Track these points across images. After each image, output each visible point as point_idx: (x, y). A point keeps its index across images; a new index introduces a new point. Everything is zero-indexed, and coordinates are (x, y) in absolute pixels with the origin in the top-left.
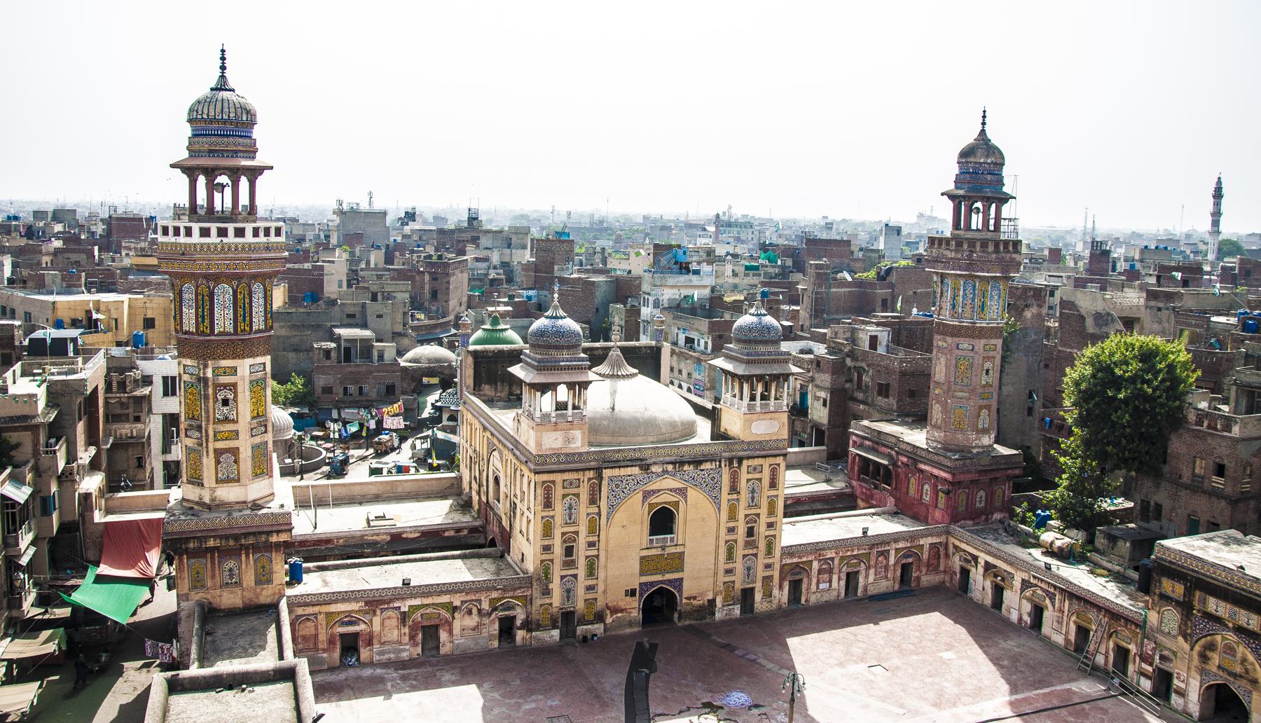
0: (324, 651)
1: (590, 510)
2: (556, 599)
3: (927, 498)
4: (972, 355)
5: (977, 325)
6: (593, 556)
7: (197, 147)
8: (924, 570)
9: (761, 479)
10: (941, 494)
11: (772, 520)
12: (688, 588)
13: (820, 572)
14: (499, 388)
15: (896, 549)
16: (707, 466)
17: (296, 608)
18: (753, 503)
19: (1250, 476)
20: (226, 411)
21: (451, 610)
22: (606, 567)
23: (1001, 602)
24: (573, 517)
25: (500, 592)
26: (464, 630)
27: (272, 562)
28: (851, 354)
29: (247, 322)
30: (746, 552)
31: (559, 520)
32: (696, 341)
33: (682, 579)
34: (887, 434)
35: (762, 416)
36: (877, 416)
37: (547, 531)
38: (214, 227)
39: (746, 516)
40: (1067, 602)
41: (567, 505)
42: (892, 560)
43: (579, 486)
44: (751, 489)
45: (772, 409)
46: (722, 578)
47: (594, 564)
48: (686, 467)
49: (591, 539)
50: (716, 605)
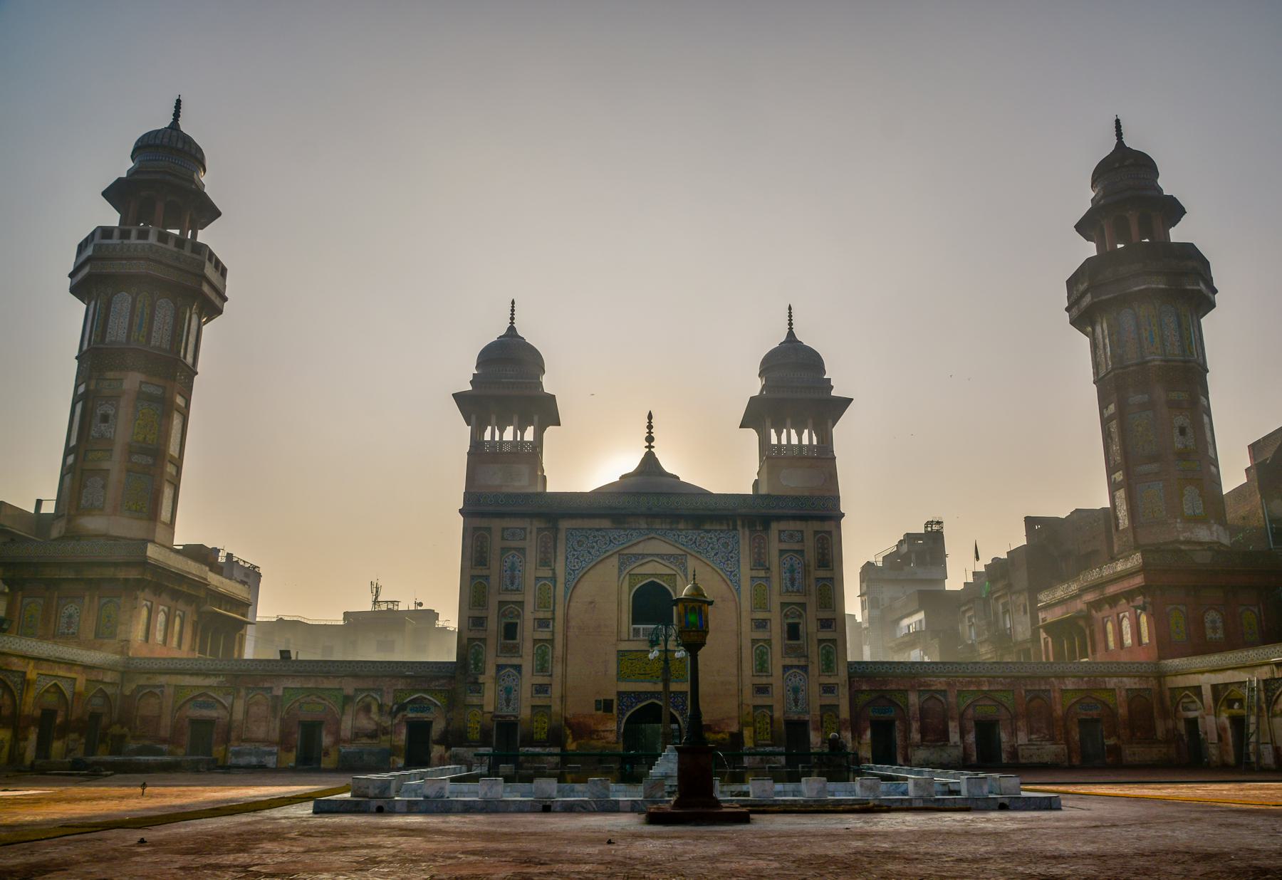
0: (164, 741)
1: (540, 574)
3: (1128, 640)
6: (546, 640)
11: (825, 615)
15: (1062, 690)
22: (564, 660)
24: (516, 584)
25: (409, 681)
30: (788, 662)
39: (783, 605)
41: (509, 564)
43: (525, 539)
44: (787, 566)
46: (750, 699)
49: (541, 615)
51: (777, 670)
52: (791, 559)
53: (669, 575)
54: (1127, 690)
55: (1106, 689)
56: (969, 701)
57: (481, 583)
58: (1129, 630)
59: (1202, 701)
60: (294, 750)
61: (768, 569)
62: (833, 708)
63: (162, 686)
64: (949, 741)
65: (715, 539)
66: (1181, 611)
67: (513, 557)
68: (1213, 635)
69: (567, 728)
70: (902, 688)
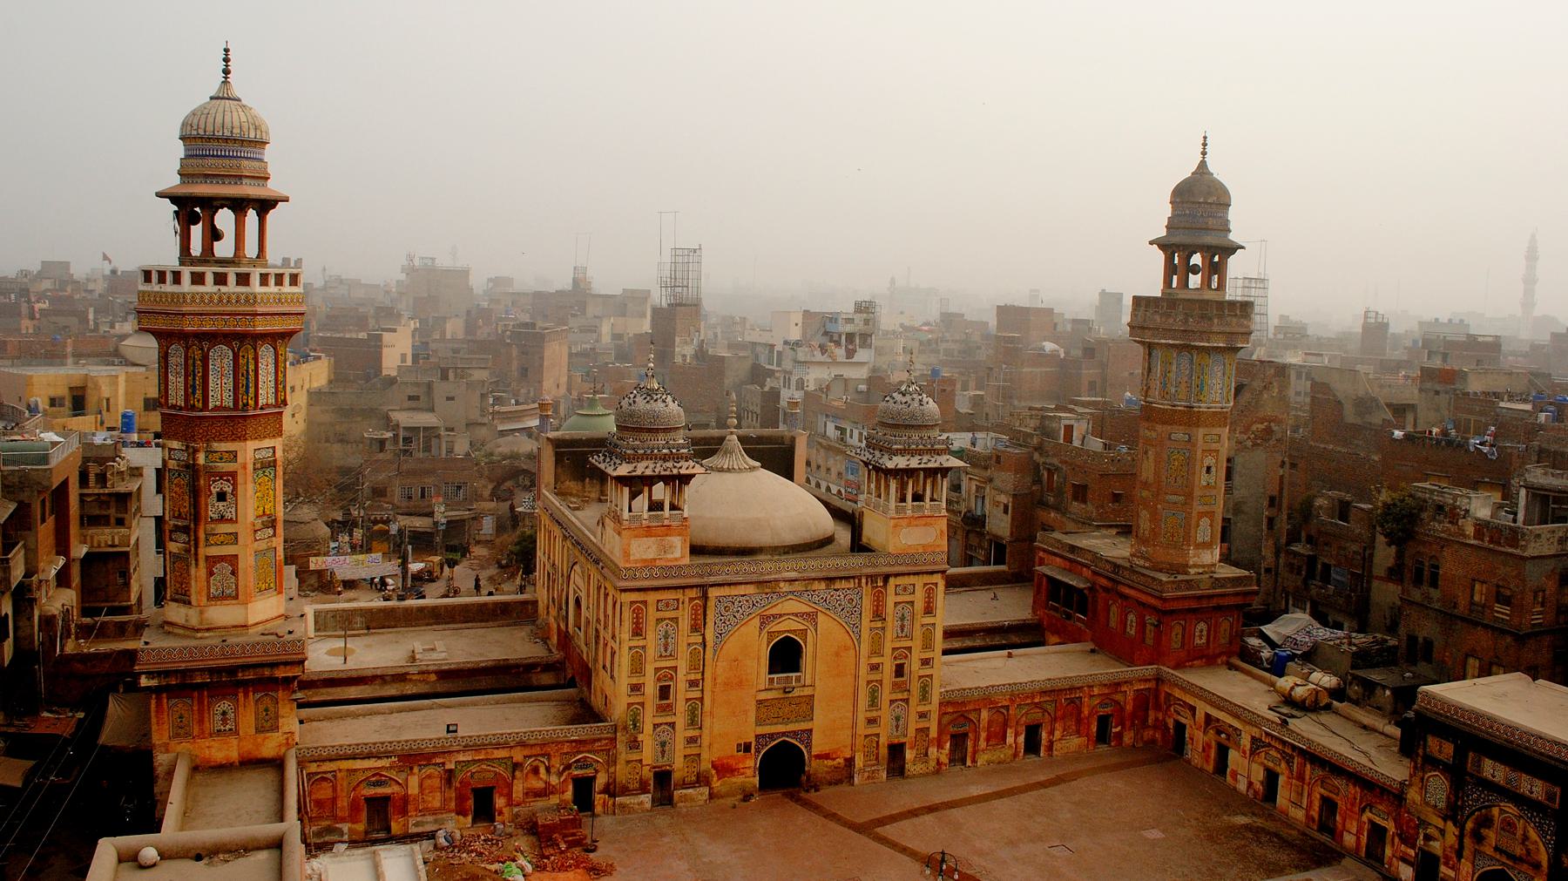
0: (343, 820)
1: (692, 640)
2: (648, 754)
3: (1132, 631)
4: (1188, 447)
7: (191, 171)
8: (1128, 724)
9: (912, 602)
10: (1149, 627)
12: (818, 745)
13: (990, 722)
14: (587, 486)
16: (844, 584)
17: (308, 764)
18: (904, 632)
19: (1543, 605)
20: (221, 508)
21: (510, 769)
23: (1226, 766)
25: (574, 744)
27: (277, 703)
28: (1039, 448)
29: (252, 393)
30: (894, 697)
32: (848, 431)
33: (811, 731)
34: (1081, 548)
36: (1071, 526)
37: (637, 667)
38: (209, 272)
40: (1308, 766)
42: (1086, 712)
43: (677, 608)
47: (696, 709)
48: (816, 585)
49: (692, 677)
51: (885, 704)
55: (1121, 692)
58: (1134, 624)
59: (1194, 715)
62: (925, 731)
65: (842, 596)
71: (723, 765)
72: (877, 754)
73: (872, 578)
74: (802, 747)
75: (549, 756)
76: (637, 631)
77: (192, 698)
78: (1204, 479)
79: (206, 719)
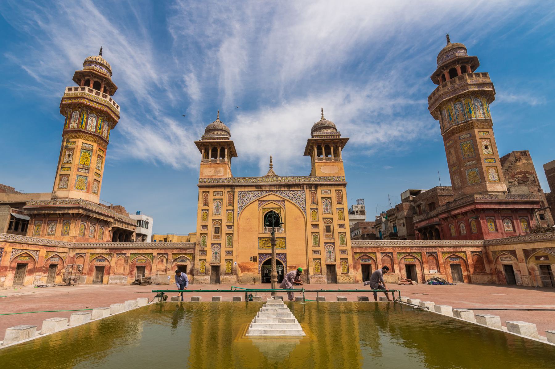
2: (209, 257)
4: (471, 139)
5: (470, 122)
12: (290, 261)
15: (443, 253)
22: (237, 241)
24: (219, 212)
25: (178, 250)
26: (158, 271)
30: (327, 241)
31: (211, 212)
33: (286, 254)
35: (327, 164)
41: (216, 205)
42: (441, 261)
43: (222, 195)
44: (325, 203)
45: (332, 161)
49: (229, 224)
50: (309, 274)
51: (322, 244)
52: (326, 201)
53: (278, 208)
54: (471, 252)
56: (402, 257)
57: (205, 212)
60: (134, 277)
61: (317, 205)
62: (345, 260)
63: (85, 253)
64: (394, 273)
65: (296, 194)
66: (492, 219)
67: (218, 202)
68: (508, 229)
69: (239, 268)
70: (374, 251)
71: (243, 266)
72: (321, 269)
73: (309, 186)
74: (282, 262)
75: (167, 254)
76: (206, 204)
77: (43, 221)
78: (485, 152)
79: (45, 229)
